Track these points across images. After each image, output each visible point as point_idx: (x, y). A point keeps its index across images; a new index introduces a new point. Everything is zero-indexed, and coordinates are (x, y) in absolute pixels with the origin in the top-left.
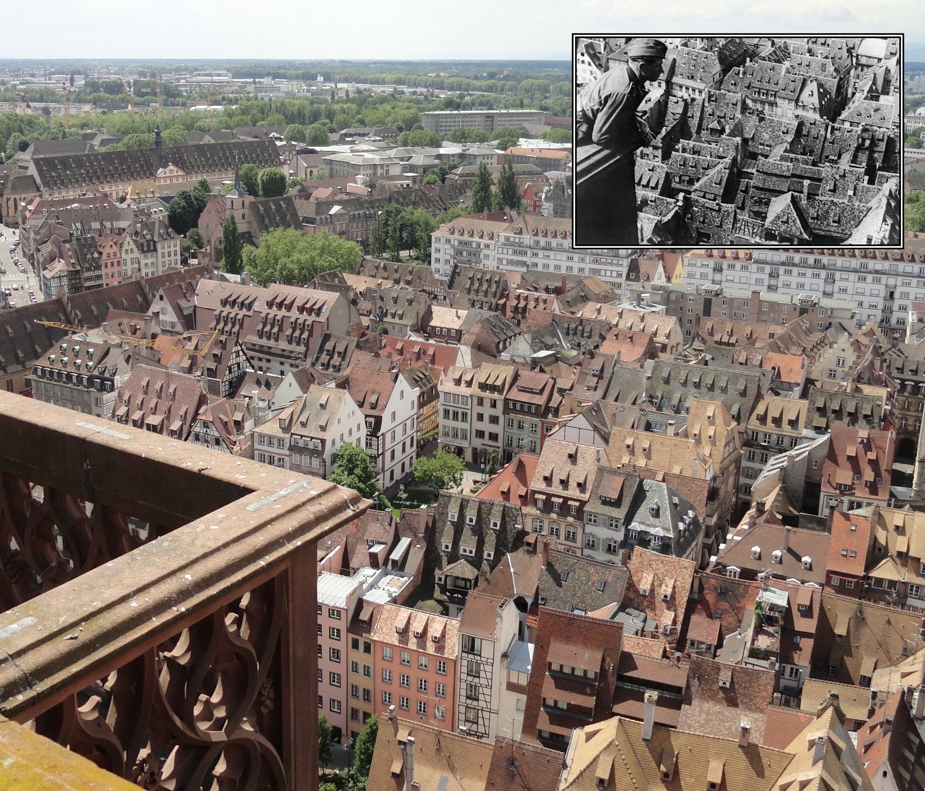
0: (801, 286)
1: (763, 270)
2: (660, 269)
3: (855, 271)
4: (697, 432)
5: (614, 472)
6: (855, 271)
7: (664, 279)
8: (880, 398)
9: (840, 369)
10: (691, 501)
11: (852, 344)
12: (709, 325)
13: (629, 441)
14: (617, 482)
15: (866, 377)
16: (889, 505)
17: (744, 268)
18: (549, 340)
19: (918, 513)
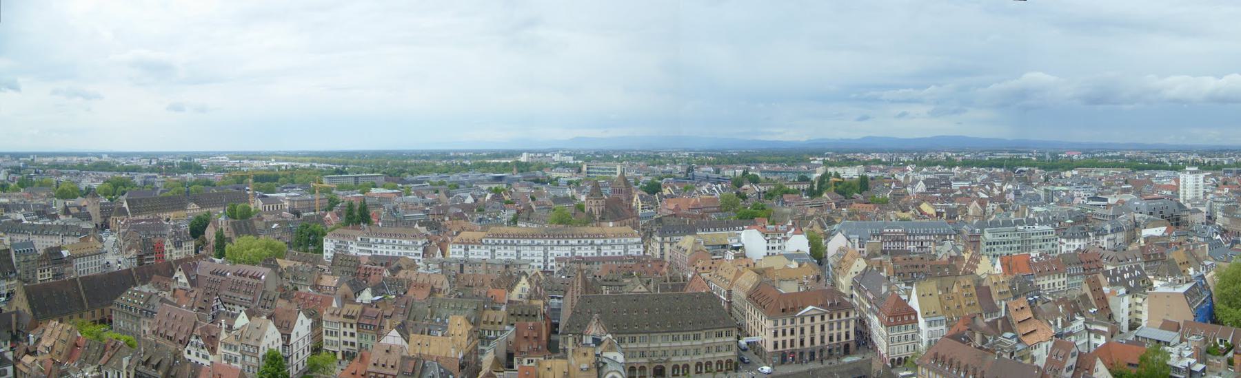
0: (506, 254)
1: (488, 248)
2: (439, 251)
3: (529, 245)
4: (453, 333)
5: (410, 358)
6: (529, 245)
7: (441, 256)
8: (540, 306)
9: (523, 294)
10: (451, 370)
11: (528, 281)
12: (462, 278)
13: (419, 342)
14: (412, 363)
15: (534, 295)
16: (545, 359)
17: (479, 248)
18: (381, 291)
19: (557, 360)
